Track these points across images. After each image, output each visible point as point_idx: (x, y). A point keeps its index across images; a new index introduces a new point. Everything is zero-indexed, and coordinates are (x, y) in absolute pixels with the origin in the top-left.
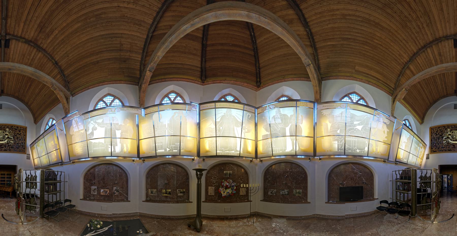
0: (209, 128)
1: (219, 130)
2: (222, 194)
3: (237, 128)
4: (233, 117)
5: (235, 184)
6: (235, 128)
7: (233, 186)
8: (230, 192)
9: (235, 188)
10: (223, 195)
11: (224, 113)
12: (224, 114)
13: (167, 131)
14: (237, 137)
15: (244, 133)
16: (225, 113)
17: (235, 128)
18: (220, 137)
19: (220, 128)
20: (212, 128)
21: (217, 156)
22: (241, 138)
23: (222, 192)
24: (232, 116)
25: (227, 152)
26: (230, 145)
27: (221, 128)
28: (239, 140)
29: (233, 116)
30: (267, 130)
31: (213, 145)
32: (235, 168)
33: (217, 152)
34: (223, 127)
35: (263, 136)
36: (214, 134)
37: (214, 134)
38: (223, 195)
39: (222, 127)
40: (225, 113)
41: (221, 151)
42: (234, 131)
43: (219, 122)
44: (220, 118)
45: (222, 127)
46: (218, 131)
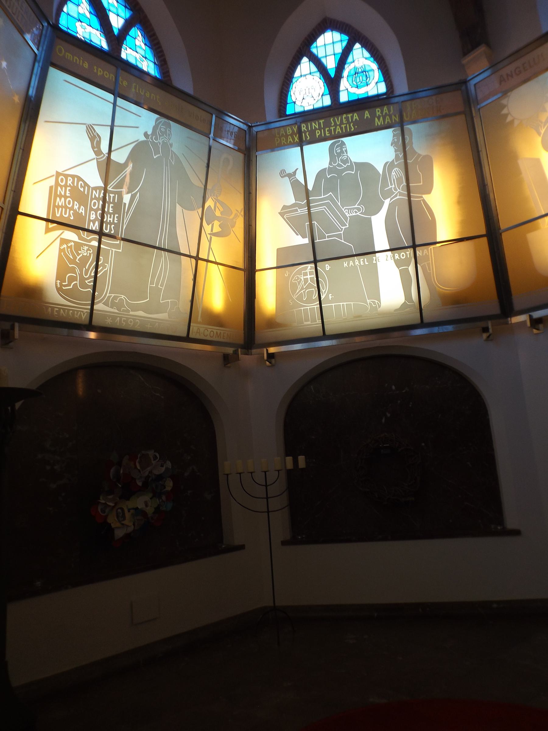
0: (73, 176)
1: (118, 206)
2: (111, 530)
5: (169, 464)
6: (179, 208)
7: (160, 477)
8: (150, 510)
9: (169, 485)
10: (119, 533)
15: (209, 236)
16: (149, 133)
17: (179, 208)
19: (121, 198)
20: (89, 186)
23: (112, 520)
25: (141, 313)
26: (152, 283)
27: (127, 198)
28: (187, 264)
30: (298, 230)
31: (78, 271)
33: (95, 307)
34: (136, 193)
35: (278, 250)
36: (93, 217)
38: (119, 533)
39: (129, 195)
40: (149, 133)
41: (112, 307)
42: (173, 224)
44: (131, 147)
45: (129, 195)
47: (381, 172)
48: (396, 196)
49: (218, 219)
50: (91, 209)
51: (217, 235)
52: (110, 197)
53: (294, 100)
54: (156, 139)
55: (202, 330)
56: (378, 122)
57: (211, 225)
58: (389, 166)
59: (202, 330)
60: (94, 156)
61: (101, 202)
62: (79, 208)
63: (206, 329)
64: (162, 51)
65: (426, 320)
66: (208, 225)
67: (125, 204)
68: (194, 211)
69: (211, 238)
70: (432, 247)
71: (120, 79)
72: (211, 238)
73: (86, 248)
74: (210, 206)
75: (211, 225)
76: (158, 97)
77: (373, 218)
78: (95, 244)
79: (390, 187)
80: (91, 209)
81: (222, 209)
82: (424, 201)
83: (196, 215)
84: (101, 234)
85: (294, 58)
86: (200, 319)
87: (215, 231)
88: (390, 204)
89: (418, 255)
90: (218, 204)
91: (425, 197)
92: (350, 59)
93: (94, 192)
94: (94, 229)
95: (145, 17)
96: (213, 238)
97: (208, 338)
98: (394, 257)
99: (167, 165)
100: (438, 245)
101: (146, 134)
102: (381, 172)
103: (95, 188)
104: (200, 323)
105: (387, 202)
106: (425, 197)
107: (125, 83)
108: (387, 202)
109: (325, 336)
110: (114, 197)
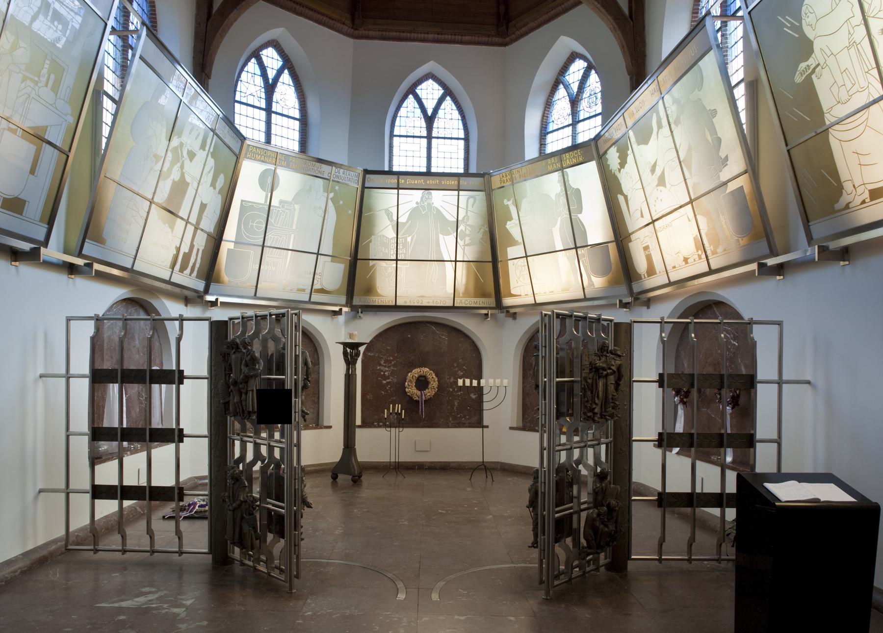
1: (405, 244)
3: (445, 236)
4: (435, 213)
6: (441, 236)
11: (417, 203)
12: (416, 205)
13: (292, 236)
14: (445, 260)
17: (441, 236)
18: (407, 262)
19: (406, 240)
21: (396, 308)
22: (456, 261)
24: (434, 210)
27: (409, 239)
28: (450, 266)
29: (436, 208)
32: (443, 335)
34: (414, 235)
36: (392, 253)
37: (392, 253)
40: (419, 201)
43: (404, 224)
44: (408, 213)
46: (401, 247)
47: (554, 200)
48: (563, 215)
49: (468, 235)
50: (391, 249)
51: (468, 245)
52: (400, 241)
53: (553, 120)
54: (423, 203)
55: (463, 301)
56: (550, 168)
57: (463, 241)
58: (558, 195)
59: (463, 301)
60: (390, 223)
61: (396, 245)
62: (385, 250)
63: (466, 300)
64: (462, 111)
65: (587, 296)
66: (461, 240)
67: (409, 242)
68: (451, 236)
69: (464, 248)
70: (586, 248)
71: (400, 180)
72: (464, 248)
73: (390, 269)
74: (462, 230)
75: (463, 241)
76: (422, 181)
77: (553, 229)
78: (395, 265)
79: (560, 209)
80: (391, 249)
81: (470, 229)
82: (578, 218)
83: (452, 238)
84: (397, 260)
85: (552, 87)
86: (461, 295)
87: (466, 243)
88: (561, 220)
89: (579, 254)
90: (467, 227)
91: (579, 215)
92: (588, 84)
93: (392, 241)
94: (393, 258)
95: (451, 91)
96: (466, 247)
97: (468, 305)
98: (566, 254)
99: (431, 215)
100: (589, 247)
101: (417, 203)
102: (554, 200)
103: (392, 239)
104: (462, 297)
105: (559, 219)
106: (579, 215)
107: (403, 181)
108: (559, 219)
109: (536, 305)
110: (402, 241)
